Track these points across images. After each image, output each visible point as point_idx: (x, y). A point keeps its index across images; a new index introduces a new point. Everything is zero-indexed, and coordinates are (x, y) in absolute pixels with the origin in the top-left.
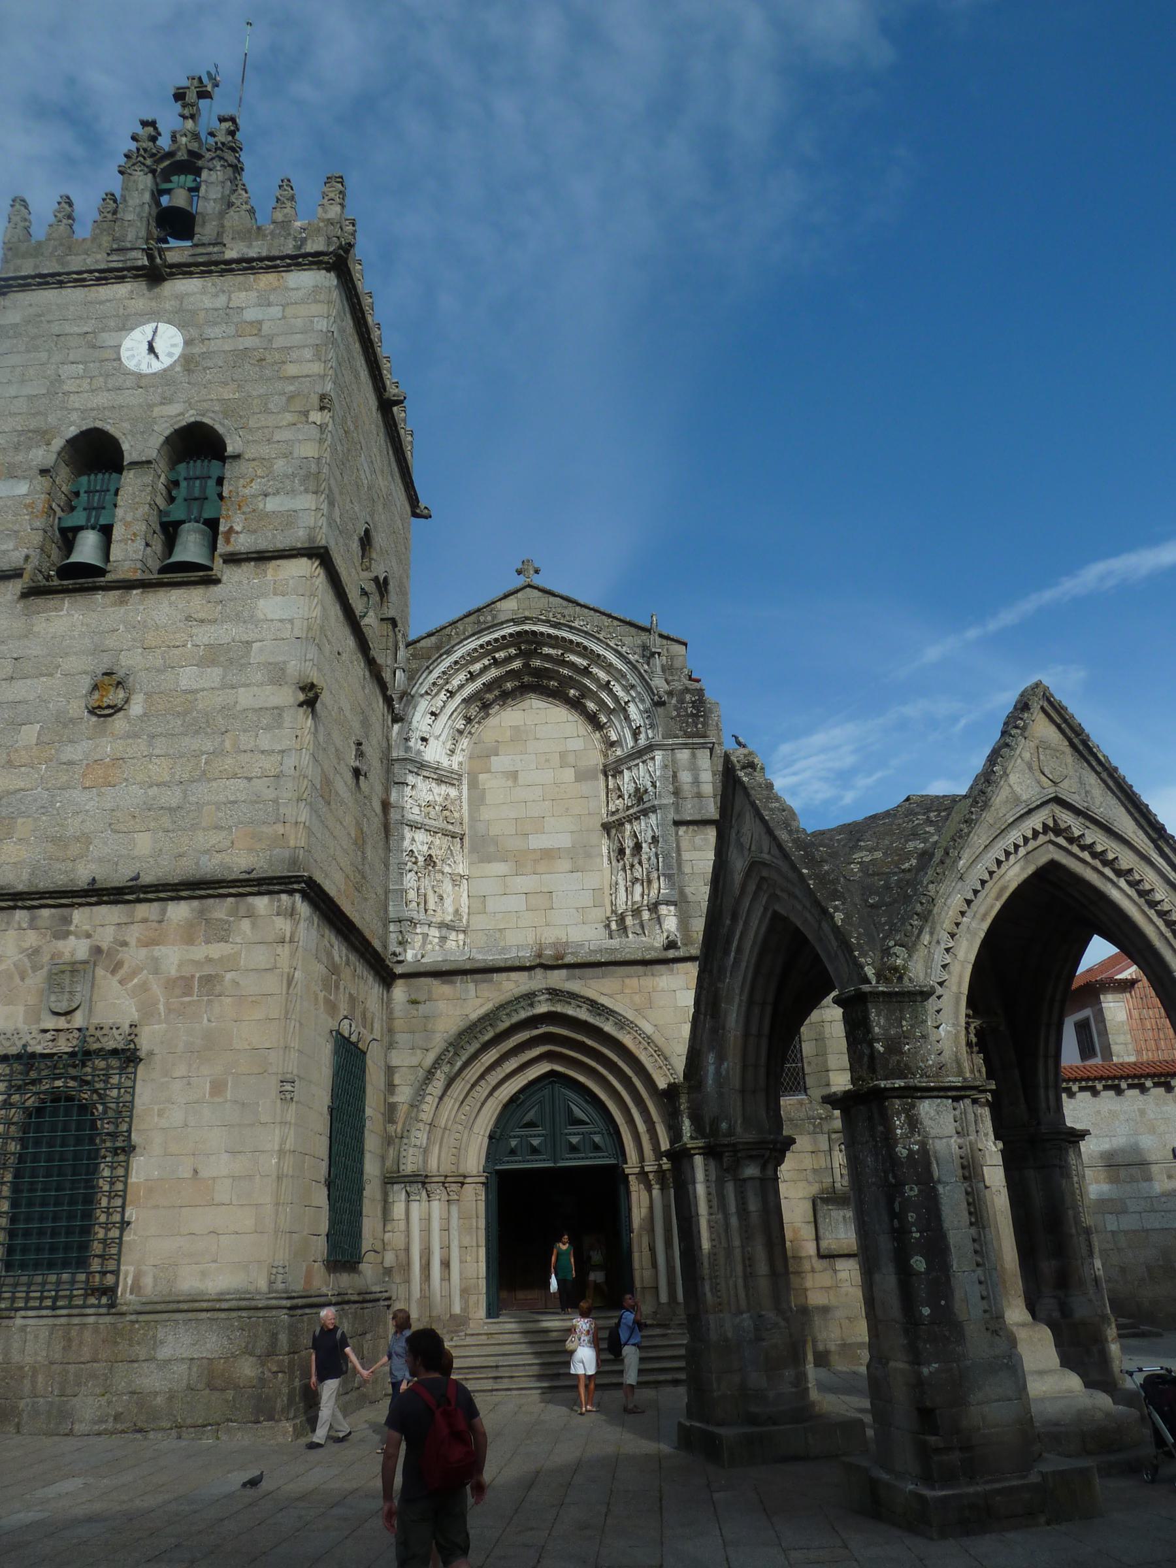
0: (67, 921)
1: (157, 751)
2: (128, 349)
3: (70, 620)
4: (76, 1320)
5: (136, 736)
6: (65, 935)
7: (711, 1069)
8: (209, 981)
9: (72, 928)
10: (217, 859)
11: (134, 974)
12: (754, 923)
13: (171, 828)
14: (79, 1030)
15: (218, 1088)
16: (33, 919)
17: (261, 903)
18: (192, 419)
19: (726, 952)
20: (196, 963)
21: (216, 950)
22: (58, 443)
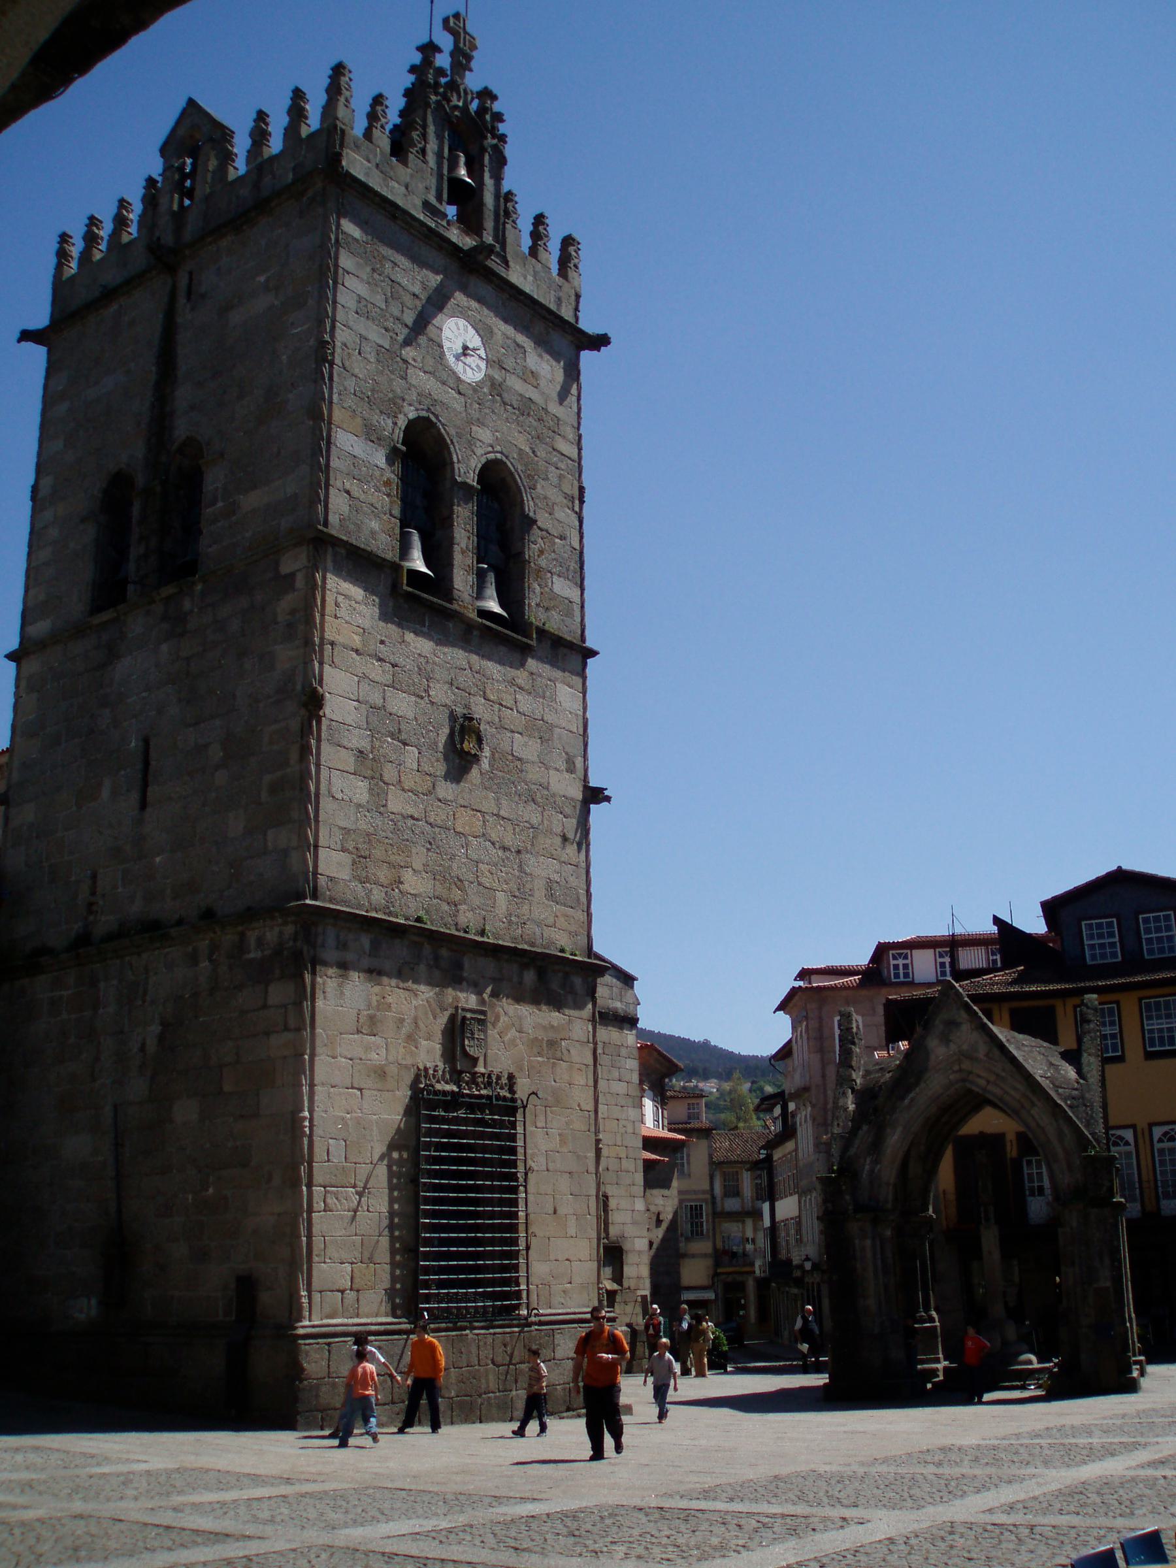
0: (459, 966)
1: (502, 813)
2: (449, 340)
7: (867, 1167)
8: (552, 1044)
9: (465, 974)
10: (547, 932)
13: (517, 894)
14: (483, 1075)
15: (563, 1140)
16: (437, 958)
19: (903, 1099)
20: (544, 1027)
22: (402, 423)
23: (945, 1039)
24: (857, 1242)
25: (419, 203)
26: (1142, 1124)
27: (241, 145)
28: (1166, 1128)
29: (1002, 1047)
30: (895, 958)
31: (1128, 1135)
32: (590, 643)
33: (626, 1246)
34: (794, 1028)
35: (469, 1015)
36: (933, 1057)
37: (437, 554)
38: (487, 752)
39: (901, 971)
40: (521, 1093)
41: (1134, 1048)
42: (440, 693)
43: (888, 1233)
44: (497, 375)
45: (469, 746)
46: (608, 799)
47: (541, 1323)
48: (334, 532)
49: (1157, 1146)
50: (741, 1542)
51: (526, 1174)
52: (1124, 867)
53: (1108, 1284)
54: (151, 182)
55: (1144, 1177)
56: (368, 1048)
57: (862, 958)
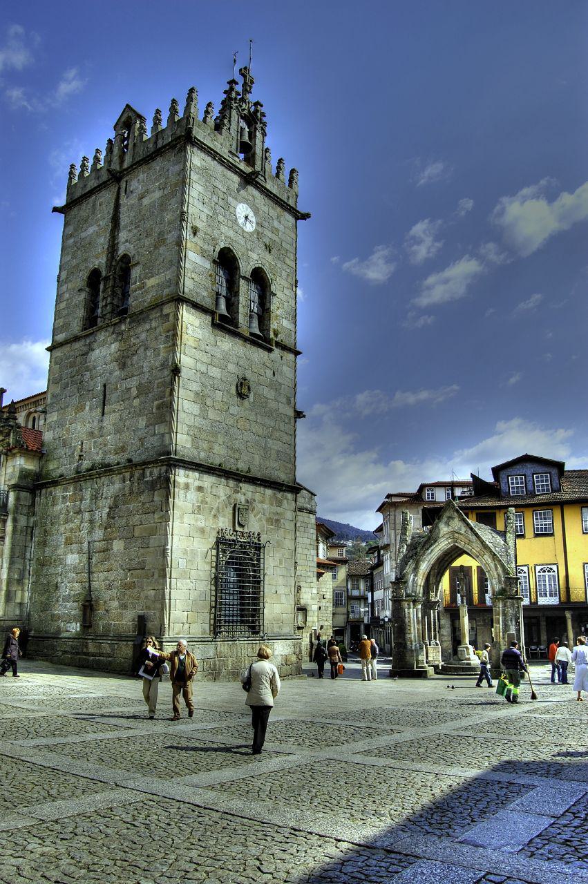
3: (227, 344)
4: (254, 642)
5: (252, 410)
6: (238, 492)
8: (277, 521)
11: (258, 513)
12: (442, 545)
15: (281, 562)
16: (227, 483)
17: (289, 496)
18: (260, 266)
19: (428, 549)
21: (279, 510)
22: (218, 249)
23: (447, 524)
24: (406, 610)
25: (226, 151)
26: (531, 565)
27: (149, 126)
28: (542, 567)
29: (471, 529)
30: (428, 491)
31: (525, 569)
32: (297, 349)
33: (308, 608)
34: (384, 520)
35: (241, 507)
36: (442, 532)
37: (232, 305)
38: (252, 394)
39: (430, 496)
40: (263, 539)
41: (529, 533)
42: (231, 367)
43: (420, 607)
44: (260, 230)
45: (245, 390)
46: (304, 416)
47: (269, 640)
48: (187, 296)
49: (538, 574)
50: (344, 739)
51: (264, 575)
52: (528, 454)
53: (514, 632)
54: (110, 141)
55: (532, 587)
56: (197, 520)
57: (413, 489)
